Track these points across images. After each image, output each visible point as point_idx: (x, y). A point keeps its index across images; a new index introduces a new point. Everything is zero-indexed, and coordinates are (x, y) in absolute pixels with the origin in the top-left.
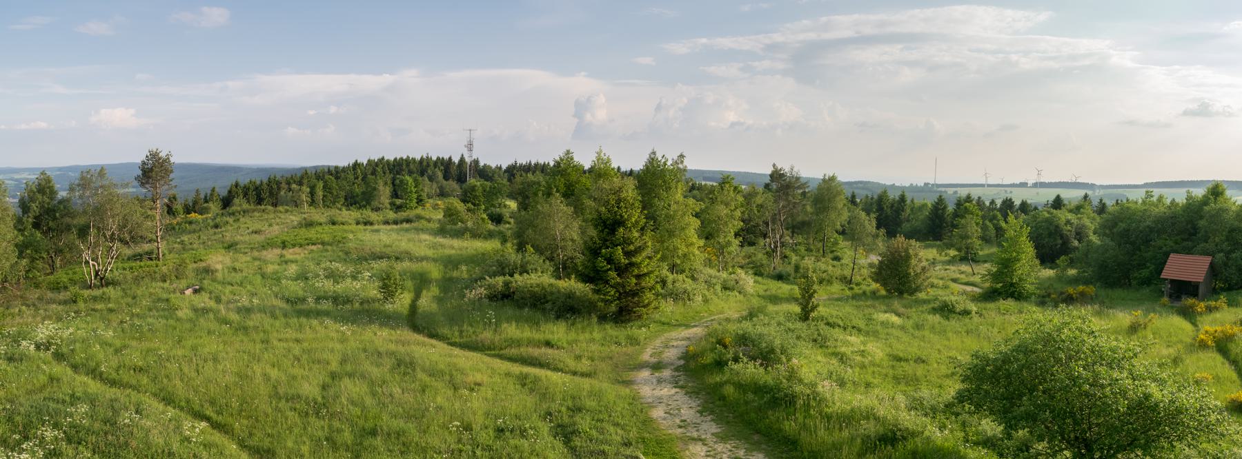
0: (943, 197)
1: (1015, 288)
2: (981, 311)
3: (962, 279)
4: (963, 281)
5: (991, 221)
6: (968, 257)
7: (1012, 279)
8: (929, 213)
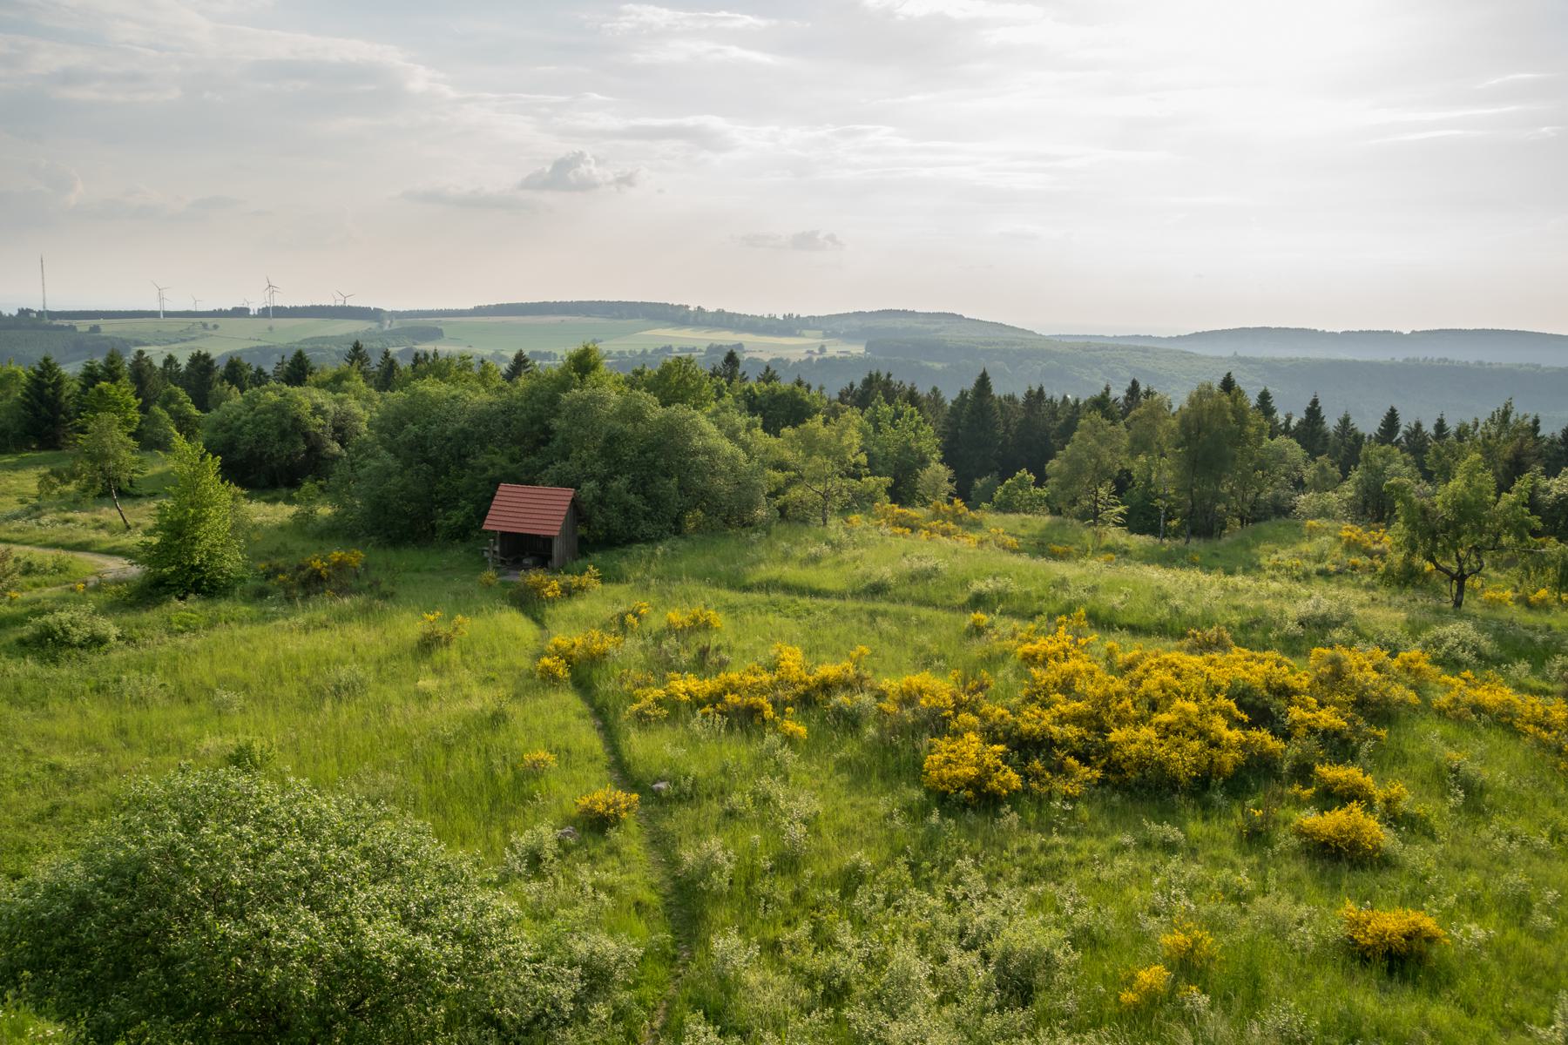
0: (52, 362)
1: (202, 572)
2: (131, 631)
3: (100, 541)
4: (104, 546)
5: (165, 405)
6: (116, 490)
7: (192, 559)
8: (24, 394)
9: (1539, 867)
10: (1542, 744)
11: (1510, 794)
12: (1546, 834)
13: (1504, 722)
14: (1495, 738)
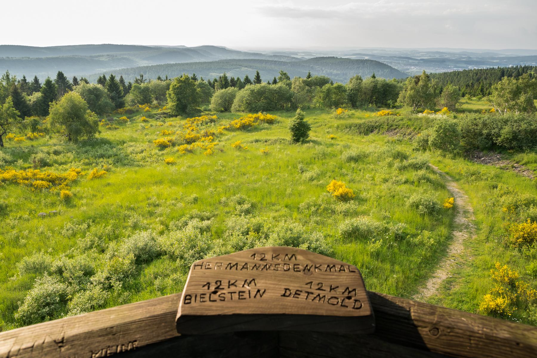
9: (26, 224)
10: (27, 185)
11: (17, 205)
12: (28, 213)
13: (14, 182)
14: (12, 188)
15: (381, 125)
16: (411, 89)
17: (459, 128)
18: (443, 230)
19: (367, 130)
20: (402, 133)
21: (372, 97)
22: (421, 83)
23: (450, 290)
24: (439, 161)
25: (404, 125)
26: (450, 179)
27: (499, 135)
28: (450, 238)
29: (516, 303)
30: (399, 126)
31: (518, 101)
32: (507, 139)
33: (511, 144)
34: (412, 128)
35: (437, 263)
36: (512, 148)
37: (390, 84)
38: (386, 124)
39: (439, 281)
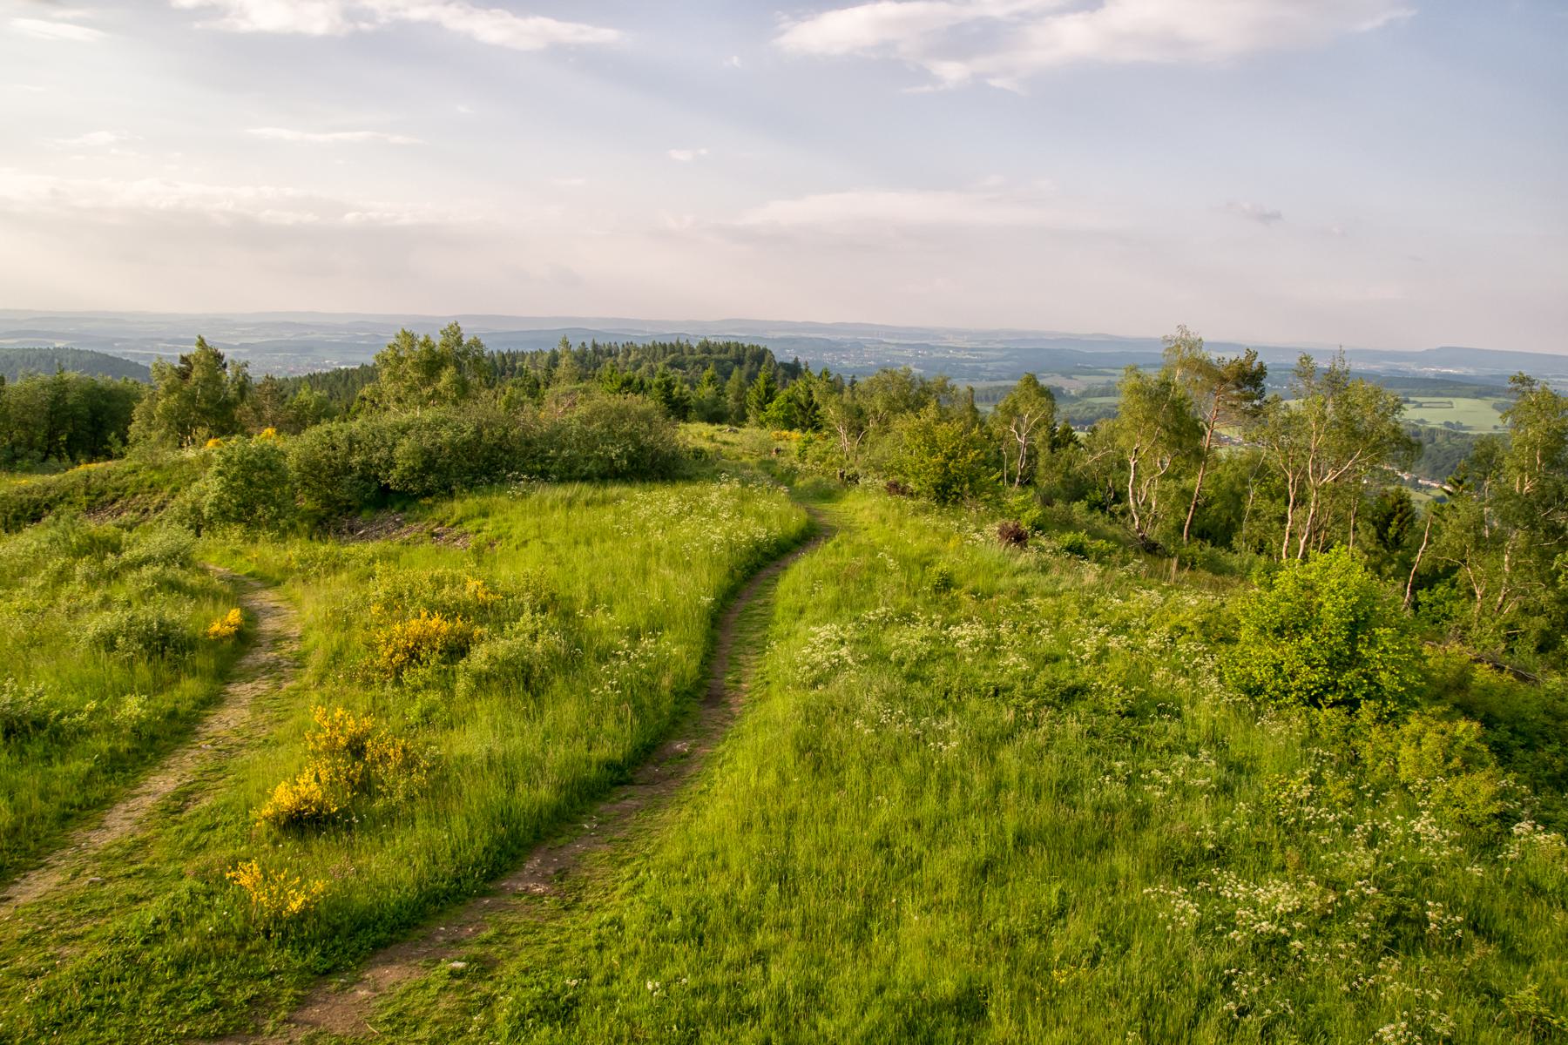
15: (66, 494)
16: (170, 391)
17: (291, 463)
18: (190, 688)
19: (17, 518)
20: (138, 510)
21: (52, 435)
22: (197, 374)
23: (181, 812)
24: (236, 553)
25: (140, 484)
26: (258, 585)
27: (392, 465)
28: (212, 701)
29: (365, 787)
30: (125, 490)
31: (440, 386)
32: (412, 469)
33: (423, 479)
34: (167, 489)
35: (151, 764)
36: (428, 493)
37: (107, 388)
38: (82, 490)
39: (148, 802)
